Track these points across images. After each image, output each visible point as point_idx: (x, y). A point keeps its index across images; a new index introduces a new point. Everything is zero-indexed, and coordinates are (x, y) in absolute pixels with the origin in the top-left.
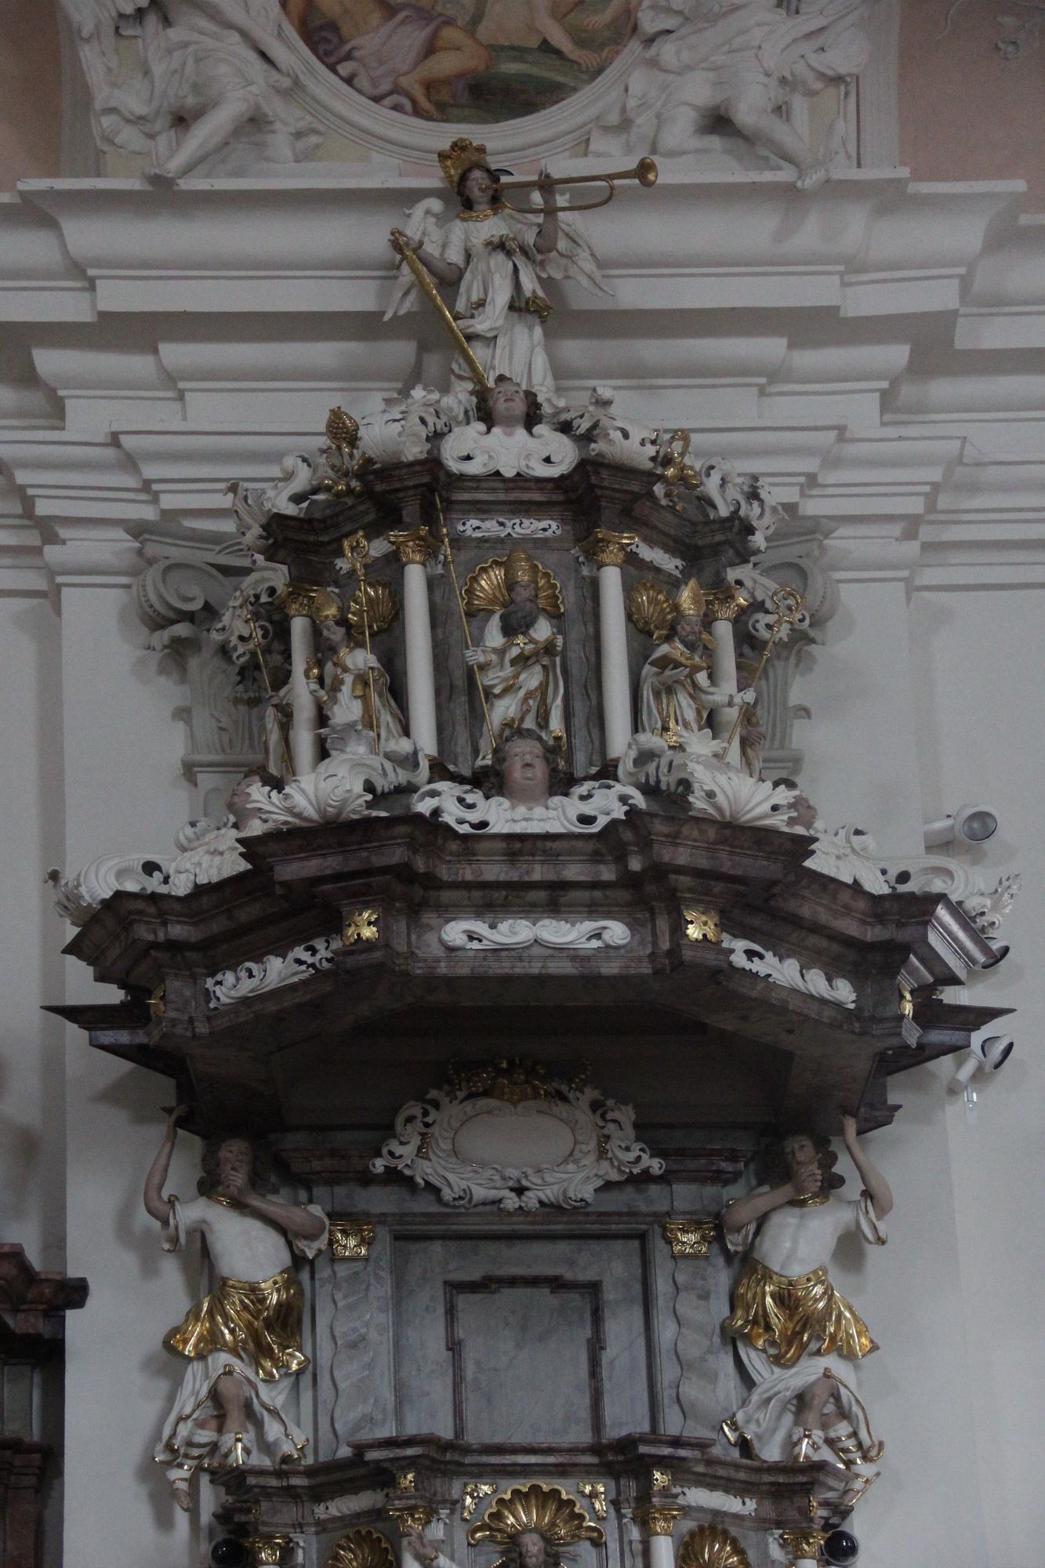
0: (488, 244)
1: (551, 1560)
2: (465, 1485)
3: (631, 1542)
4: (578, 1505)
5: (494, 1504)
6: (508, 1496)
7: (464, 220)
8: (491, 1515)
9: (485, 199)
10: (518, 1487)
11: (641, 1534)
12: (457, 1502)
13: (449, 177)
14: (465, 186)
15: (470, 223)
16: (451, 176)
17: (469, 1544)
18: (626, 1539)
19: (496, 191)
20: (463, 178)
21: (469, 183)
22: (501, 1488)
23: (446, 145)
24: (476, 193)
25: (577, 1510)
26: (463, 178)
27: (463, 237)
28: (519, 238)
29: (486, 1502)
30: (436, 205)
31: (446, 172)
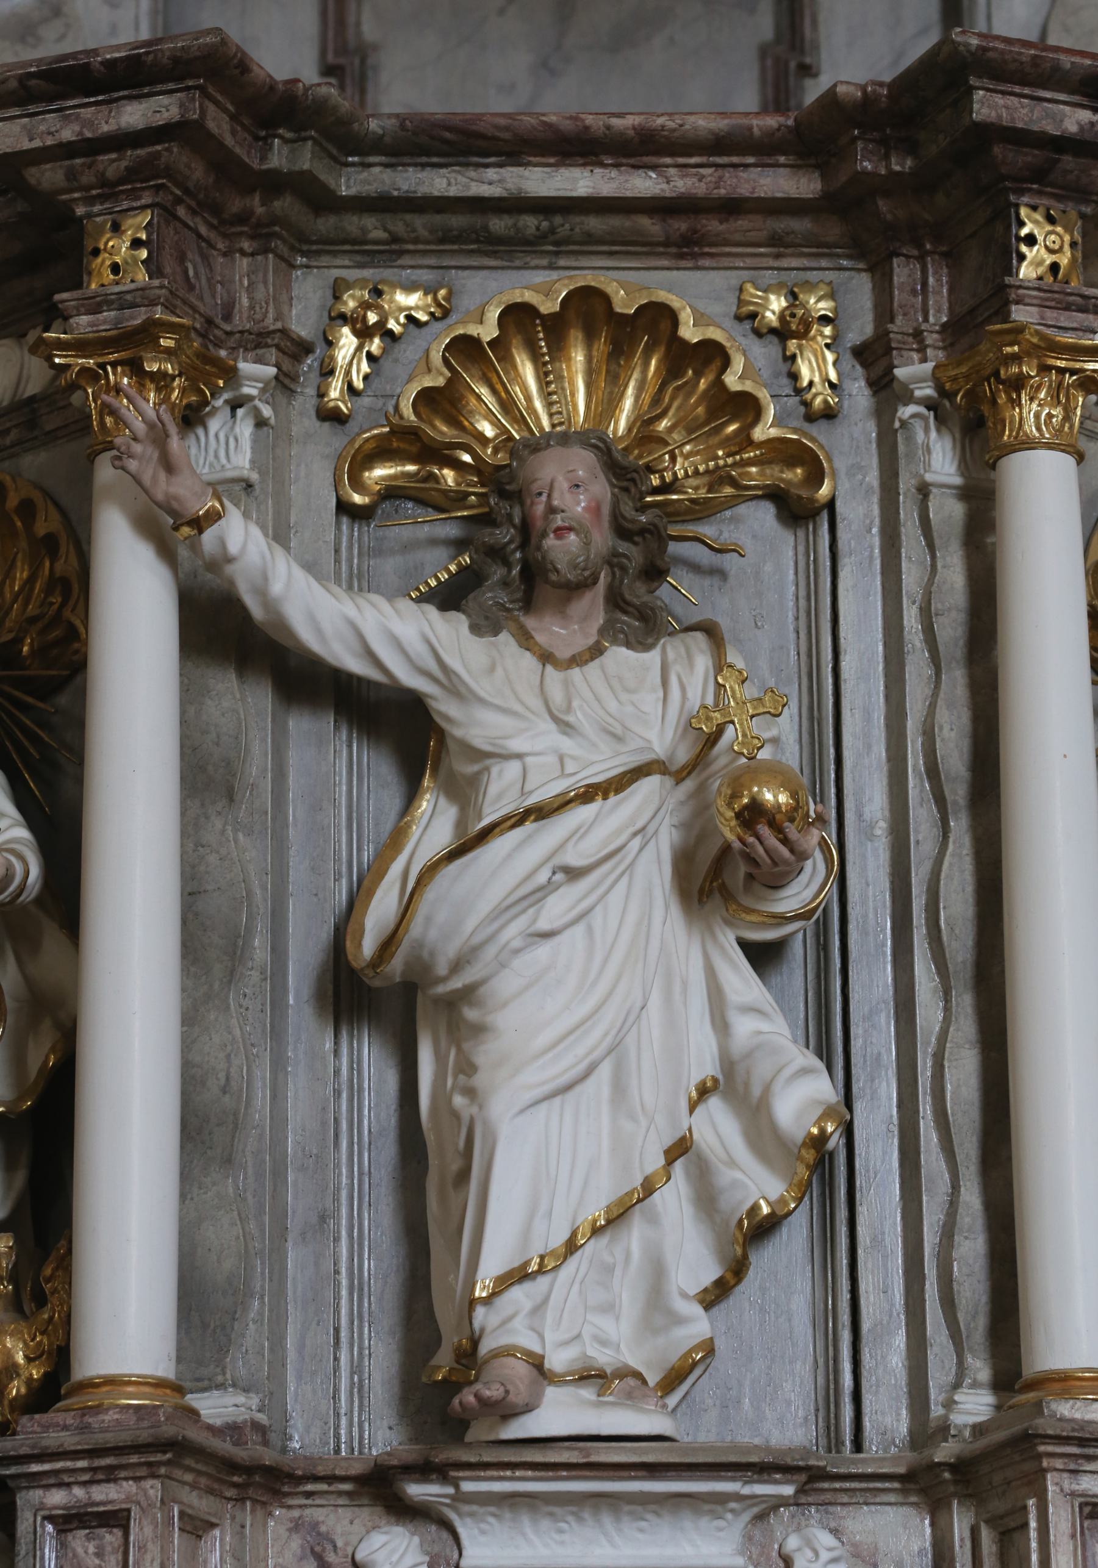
1: (634, 554)
2: (337, 291)
3: (924, 490)
4: (738, 363)
5: (436, 357)
6: (488, 331)
8: (427, 398)
10: (529, 297)
11: (964, 466)
12: (305, 348)
17: (344, 508)
18: (906, 484)
22: (467, 302)
25: (732, 381)
29: (409, 352)
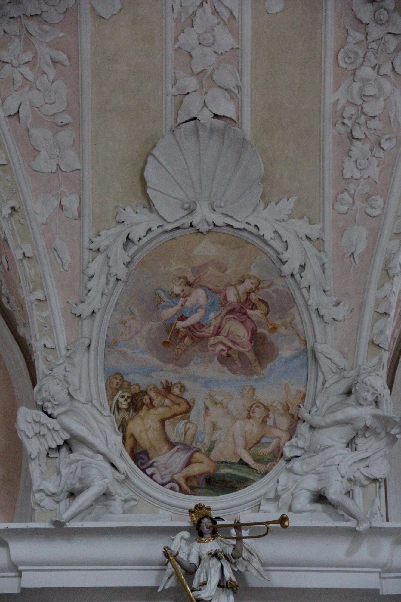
0: (210, 554)
7: (199, 542)
9: (209, 532)
13: (193, 522)
14: (200, 526)
15: (201, 543)
16: (194, 521)
19: (214, 528)
20: (200, 522)
21: (202, 525)
23: (192, 506)
24: (205, 529)
26: (200, 522)
27: (198, 550)
28: (225, 551)
30: (186, 534)
31: (192, 519)
